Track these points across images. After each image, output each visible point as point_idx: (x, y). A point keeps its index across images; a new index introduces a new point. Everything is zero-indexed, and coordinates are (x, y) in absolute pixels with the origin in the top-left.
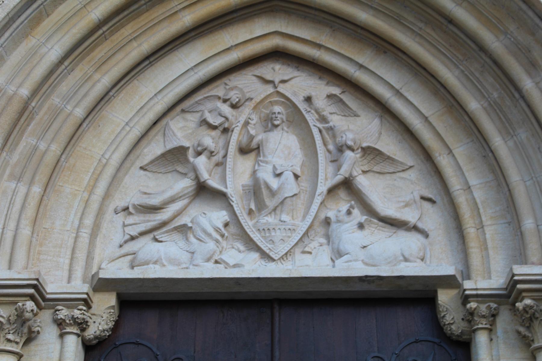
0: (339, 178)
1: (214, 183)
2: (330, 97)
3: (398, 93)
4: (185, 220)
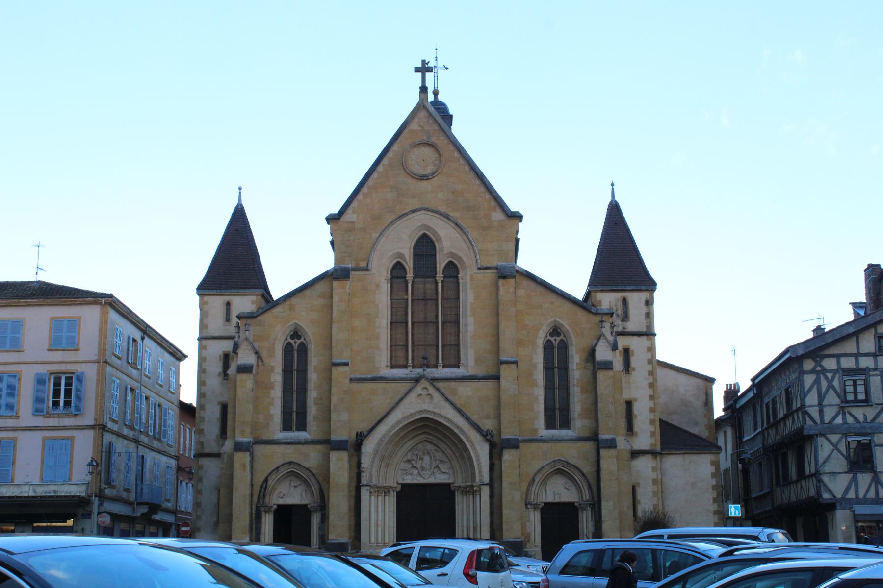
0: (436, 465)
1: (416, 466)
3: (446, 450)
4: (410, 473)
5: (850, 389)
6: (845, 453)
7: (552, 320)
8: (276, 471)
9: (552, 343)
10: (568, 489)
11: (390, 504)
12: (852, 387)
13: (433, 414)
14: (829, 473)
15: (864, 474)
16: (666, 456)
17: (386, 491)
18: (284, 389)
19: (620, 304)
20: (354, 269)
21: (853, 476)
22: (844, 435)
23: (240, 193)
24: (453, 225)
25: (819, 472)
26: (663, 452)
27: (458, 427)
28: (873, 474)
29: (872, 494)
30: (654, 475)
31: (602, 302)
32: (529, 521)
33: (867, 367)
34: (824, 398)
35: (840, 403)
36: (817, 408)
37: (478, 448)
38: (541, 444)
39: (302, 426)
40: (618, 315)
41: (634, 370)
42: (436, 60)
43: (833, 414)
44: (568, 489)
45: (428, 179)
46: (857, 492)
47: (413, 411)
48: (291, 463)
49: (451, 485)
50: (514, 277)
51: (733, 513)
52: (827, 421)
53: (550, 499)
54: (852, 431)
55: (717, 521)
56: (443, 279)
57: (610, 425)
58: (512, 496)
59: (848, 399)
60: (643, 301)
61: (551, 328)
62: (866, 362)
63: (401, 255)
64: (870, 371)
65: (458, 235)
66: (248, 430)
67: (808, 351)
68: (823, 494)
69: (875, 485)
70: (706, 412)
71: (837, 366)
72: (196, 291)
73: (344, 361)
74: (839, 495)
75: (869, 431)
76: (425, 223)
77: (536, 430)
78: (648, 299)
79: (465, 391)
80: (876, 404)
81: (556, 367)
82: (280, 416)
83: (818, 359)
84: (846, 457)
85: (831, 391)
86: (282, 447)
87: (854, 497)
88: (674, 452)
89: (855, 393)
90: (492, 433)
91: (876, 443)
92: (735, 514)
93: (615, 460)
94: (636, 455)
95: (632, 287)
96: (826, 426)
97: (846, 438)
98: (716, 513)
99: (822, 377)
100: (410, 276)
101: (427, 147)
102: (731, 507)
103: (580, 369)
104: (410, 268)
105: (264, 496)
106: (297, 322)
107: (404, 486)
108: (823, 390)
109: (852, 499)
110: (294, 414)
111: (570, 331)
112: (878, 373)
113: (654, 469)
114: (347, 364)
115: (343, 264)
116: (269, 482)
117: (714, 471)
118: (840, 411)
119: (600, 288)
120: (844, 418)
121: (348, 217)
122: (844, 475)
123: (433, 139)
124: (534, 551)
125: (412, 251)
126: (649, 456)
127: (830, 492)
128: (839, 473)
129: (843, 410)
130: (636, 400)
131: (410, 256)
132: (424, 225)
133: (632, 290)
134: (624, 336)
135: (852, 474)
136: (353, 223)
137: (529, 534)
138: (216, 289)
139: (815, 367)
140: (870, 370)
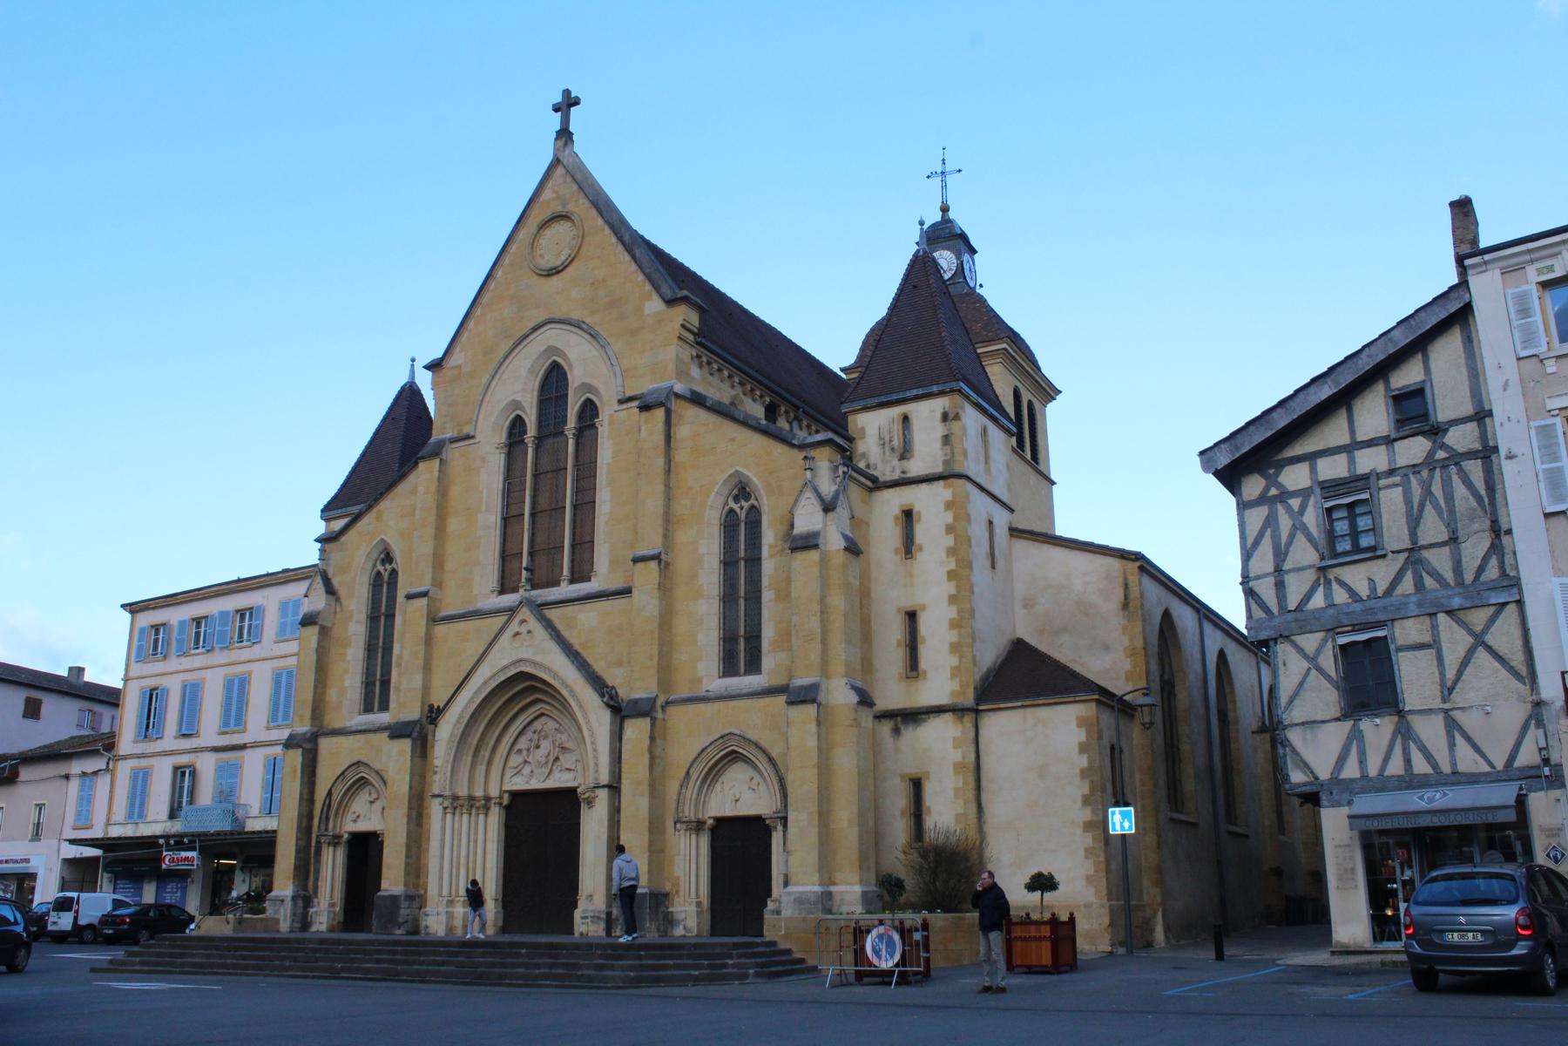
2: (556, 729)
5: (1342, 527)
6: (1333, 674)
7: (732, 471)
8: (342, 777)
9: (737, 515)
10: (754, 790)
11: (491, 828)
12: (1346, 522)
13: (532, 665)
14: (1303, 724)
15: (1378, 720)
16: (990, 714)
17: (475, 805)
18: (369, 646)
19: (897, 428)
20: (454, 440)
21: (1354, 725)
22: (1330, 634)
23: (413, 365)
24: (589, 337)
25: (1282, 723)
26: (981, 708)
27: (567, 686)
28: (1395, 719)
29: (1396, 767)
30: (956, 755)
31: (867, 429)
32: (679, 855)
33: (1371, 471)
34: (1286, 554)
35: (1318, 561)
36: (1271, 580)
37: (593, 718)
38: (703, 707)
39: (384, 706)
40: (893, 449)
41: (920, 549)
42: (944, 163)
43: (1306, 588)
44: (754, 790)
45: (559, 272)
46: (1362, 762)
47: (505, 662)
48: (358, 763)
49: (579, 790)
50: (661, 404)
51: (1118, 827)
52: (1292, 606)
53: (729, 811)
54: (1346, 622)
55: (1091, 845)
56: (574, 431)
57: (812, 657)
58: (636, 803)
59: (1340, 549)
60: (939, 416)
61: (736, 486)
62: (1370, 461)
63: (516, 404)
64: (1378, 479)
65: (596, 353)
66: (308, 713)
67: (1237, 455)
68: (1290, 774)
69: (1403, 744)
70: (1126, 622)
71: (1311, 479)
72: (319, 514)
73: (423, 589)
74: (1324, 774)
75: (1381, 617)
76: (551, 343)
77: (699, 680)
78: (947, 409)
79: (585, 623)
80: (1393, 552)
81: (741, 558)
82: (359, 690)
83: (1271, 471)
84: (1337, 682)
85: (1300, 537)
86: (352, 737)
87: (1358, 775)
88: (1002, 706)
89: (1354, 534)
90: (613, 692)
91: (1400, 642)
92: (1122, 827)
93: (813, 727)
94: (923, 716)
95: (914, 392)
96: (1290, 617)
97: (1334, 640)
98: (1088, 826)
99: (1280, 508)
100: (532, 431)
101: (562, 222)
102: (1113, 813)
103: (771, 556)
104: (531, 423)
105: (327, 818)
106: (384, 537)
107: (516, 796)
108: (1284, 538)
109: (1352, 781)
110: (378, 684)
111: (760, 486)
112: (1397, 479)
113: (957, 743)
114: (424, 594)
115: (443, 434)
116: (334, 797)
117: (1083, 738)
118: (1318, 578)
119: (863, 403)
120: (1328, 595)
121: (457, 358)
122: (1333, 724)
123: (571, 207)
124: (686, 911)
125: (535, 394)
126: (949, 717)
127: (1305, 766)
128: (1323, 722)
129: (1325, 577)
130: (924, 607)
131: (532, 403)
132: (550, 347)
133: (917, 398)
134: (903, 488)
135: (1352, 722)
136: (459, 367)
137: (678, 878)
138: (341, 508)
139: (1267, 489)
140: (1379, 476)
